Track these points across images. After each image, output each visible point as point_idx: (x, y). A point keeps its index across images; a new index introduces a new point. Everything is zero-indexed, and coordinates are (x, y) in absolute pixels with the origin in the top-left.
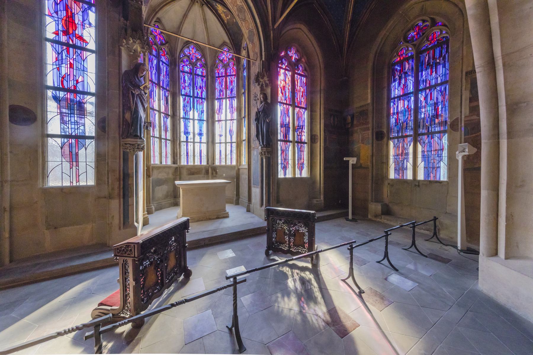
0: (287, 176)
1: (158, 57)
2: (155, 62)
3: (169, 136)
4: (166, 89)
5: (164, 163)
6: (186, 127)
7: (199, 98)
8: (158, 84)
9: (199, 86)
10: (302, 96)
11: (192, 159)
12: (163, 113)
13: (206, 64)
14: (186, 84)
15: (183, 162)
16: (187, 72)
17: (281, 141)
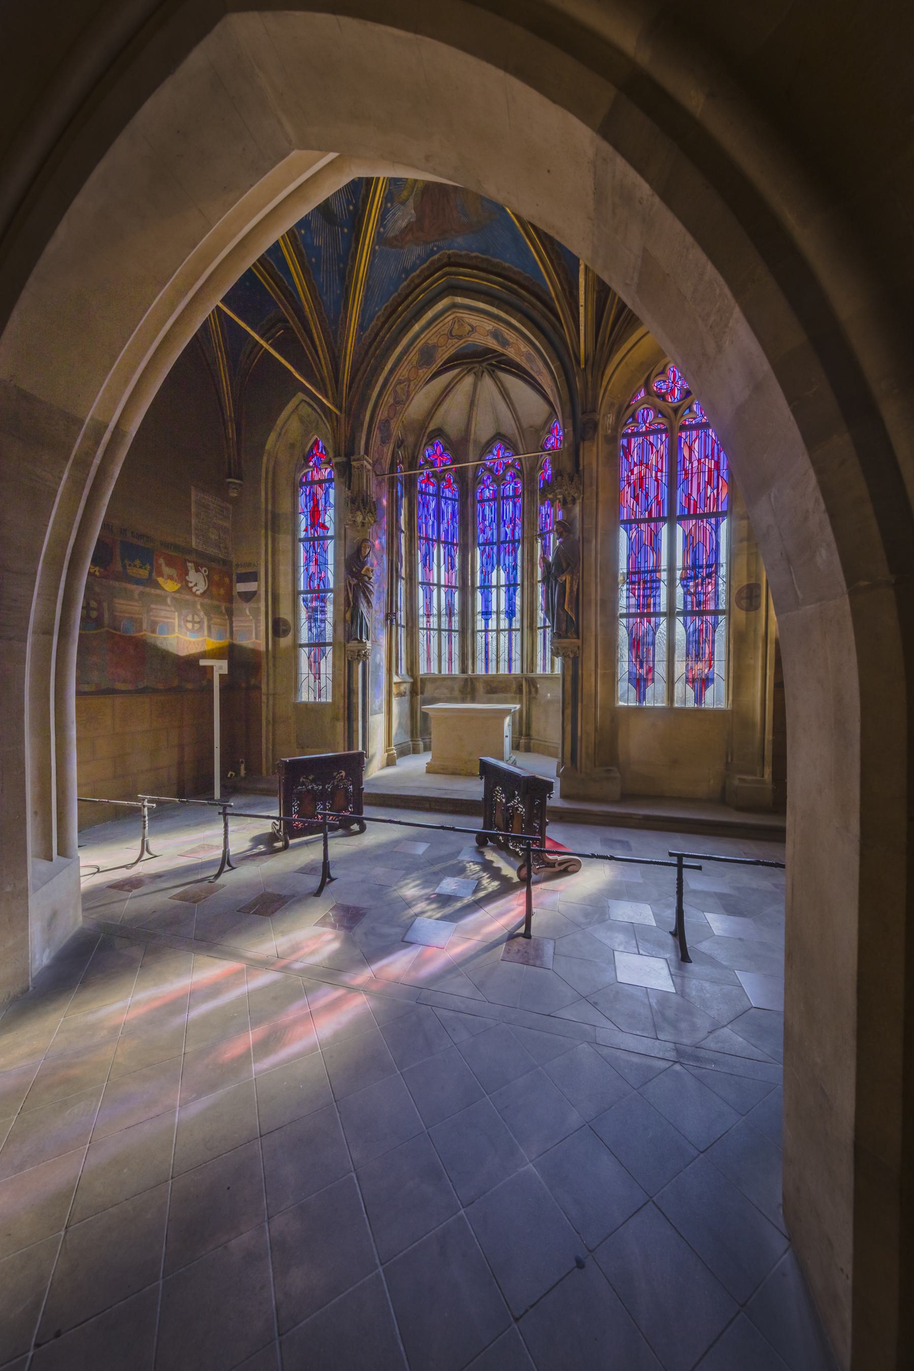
0: (647, 704)
1: (438, 495)
2: (433, 505)
3: (456, 625)
4: (452, 544)
5: (445, 671)
6: (487, 601)
7: (509, 542)
8: (438, 540)
9: (508, 519)
10: (709, 483)
11: (494, 663)
12: (445, 586)
13: (521, 471)
14: (487, 523)
15: (480, 670)
16: (489, 500)
17: (628, 616)
